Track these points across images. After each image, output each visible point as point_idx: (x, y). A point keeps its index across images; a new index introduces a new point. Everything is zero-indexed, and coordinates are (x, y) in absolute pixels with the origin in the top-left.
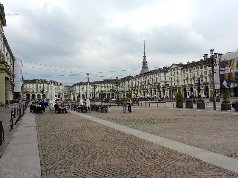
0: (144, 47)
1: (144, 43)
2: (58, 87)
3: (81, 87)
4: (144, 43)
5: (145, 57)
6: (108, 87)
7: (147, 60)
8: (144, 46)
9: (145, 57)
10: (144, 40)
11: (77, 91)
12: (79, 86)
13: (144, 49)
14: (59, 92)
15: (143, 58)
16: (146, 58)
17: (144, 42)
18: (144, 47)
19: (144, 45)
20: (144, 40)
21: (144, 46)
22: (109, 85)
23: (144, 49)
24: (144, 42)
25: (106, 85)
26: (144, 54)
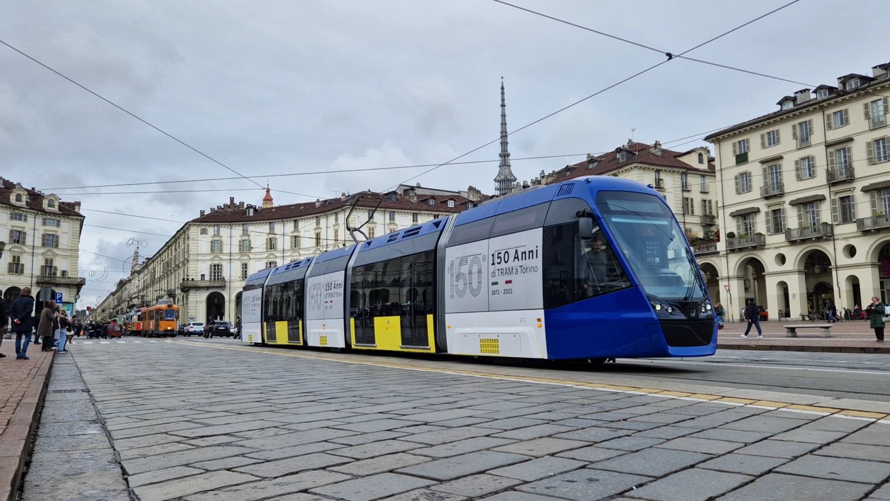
0: (504, 116)
1: (503, 100)
2: (41, 229)
3: (231, 235)
4: (503, 100)
8: (503, 111)
10: (503, 88)
11: (199, 270)
13: (504, 124)
14: (48, 266)
17: (503, 93)
18: (504, 116)
19: (503, 106)
20: (503, 88)
21: (503, 111)
23: (504, 124)
24: (503, 93)
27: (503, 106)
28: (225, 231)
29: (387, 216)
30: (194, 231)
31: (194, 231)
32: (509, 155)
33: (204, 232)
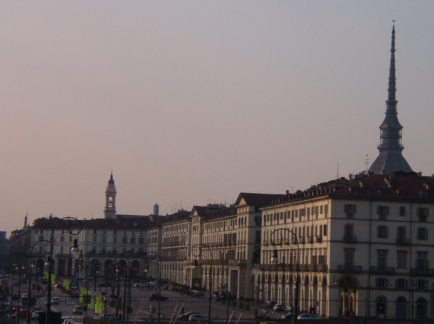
0: (393, 61)
1: (393, 44)
3: (47, 234)
4: (393, 44)
5: (392, 103)
6: (125, 240)
7: (401, 118)
9: (392, 103)
10: (393, 32)
12: (39, 232)
15: (384, 108)
16: (399, 108)
17: (393, 38)
18: (393, 61)
19: (393, 50)
20: (393, 32)
22: (129, 234)
25: (121, 234)
26: (392, 90)
27: (393, 50)
28: (45, 232)
29: (102, 232)
30: (33, 232)
31: (33, 232)
32: (397, 102)
33: (37, 232)
